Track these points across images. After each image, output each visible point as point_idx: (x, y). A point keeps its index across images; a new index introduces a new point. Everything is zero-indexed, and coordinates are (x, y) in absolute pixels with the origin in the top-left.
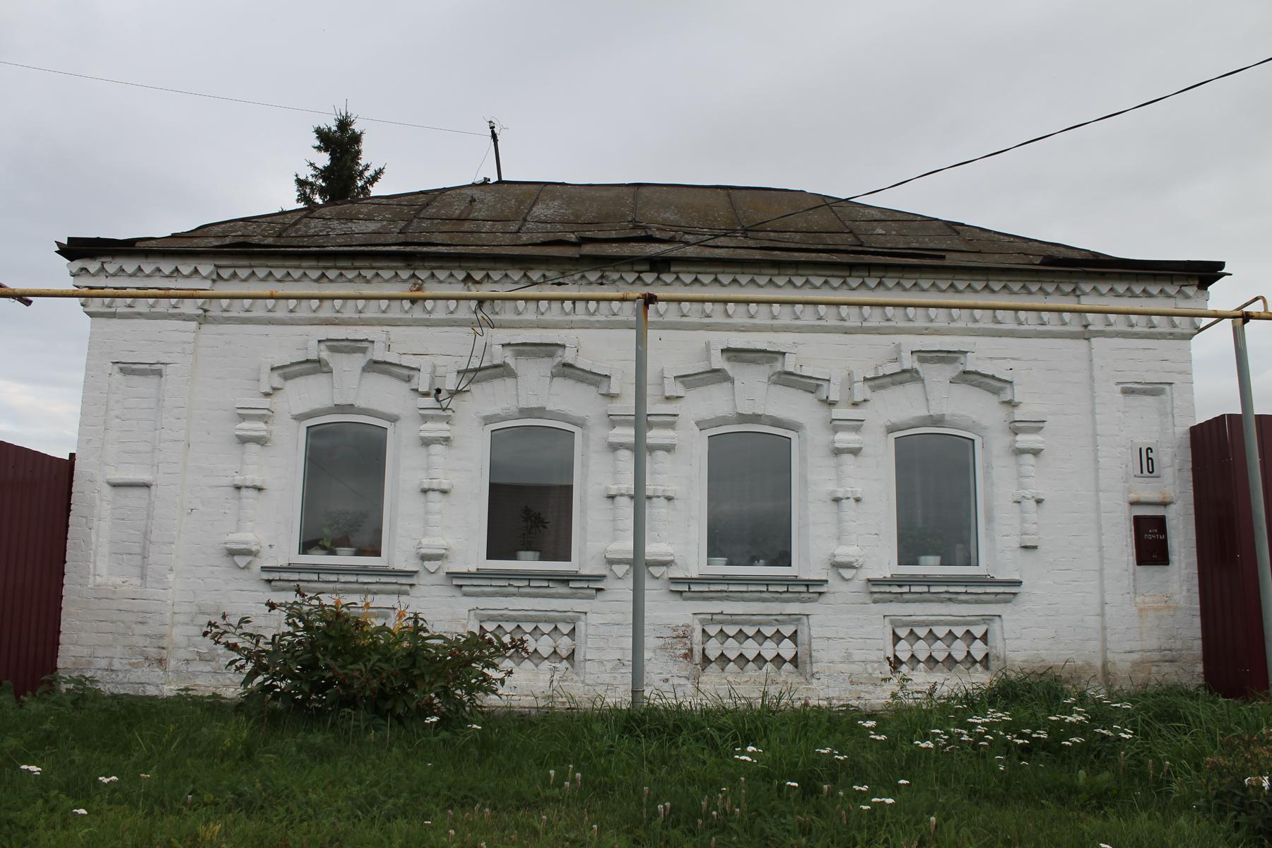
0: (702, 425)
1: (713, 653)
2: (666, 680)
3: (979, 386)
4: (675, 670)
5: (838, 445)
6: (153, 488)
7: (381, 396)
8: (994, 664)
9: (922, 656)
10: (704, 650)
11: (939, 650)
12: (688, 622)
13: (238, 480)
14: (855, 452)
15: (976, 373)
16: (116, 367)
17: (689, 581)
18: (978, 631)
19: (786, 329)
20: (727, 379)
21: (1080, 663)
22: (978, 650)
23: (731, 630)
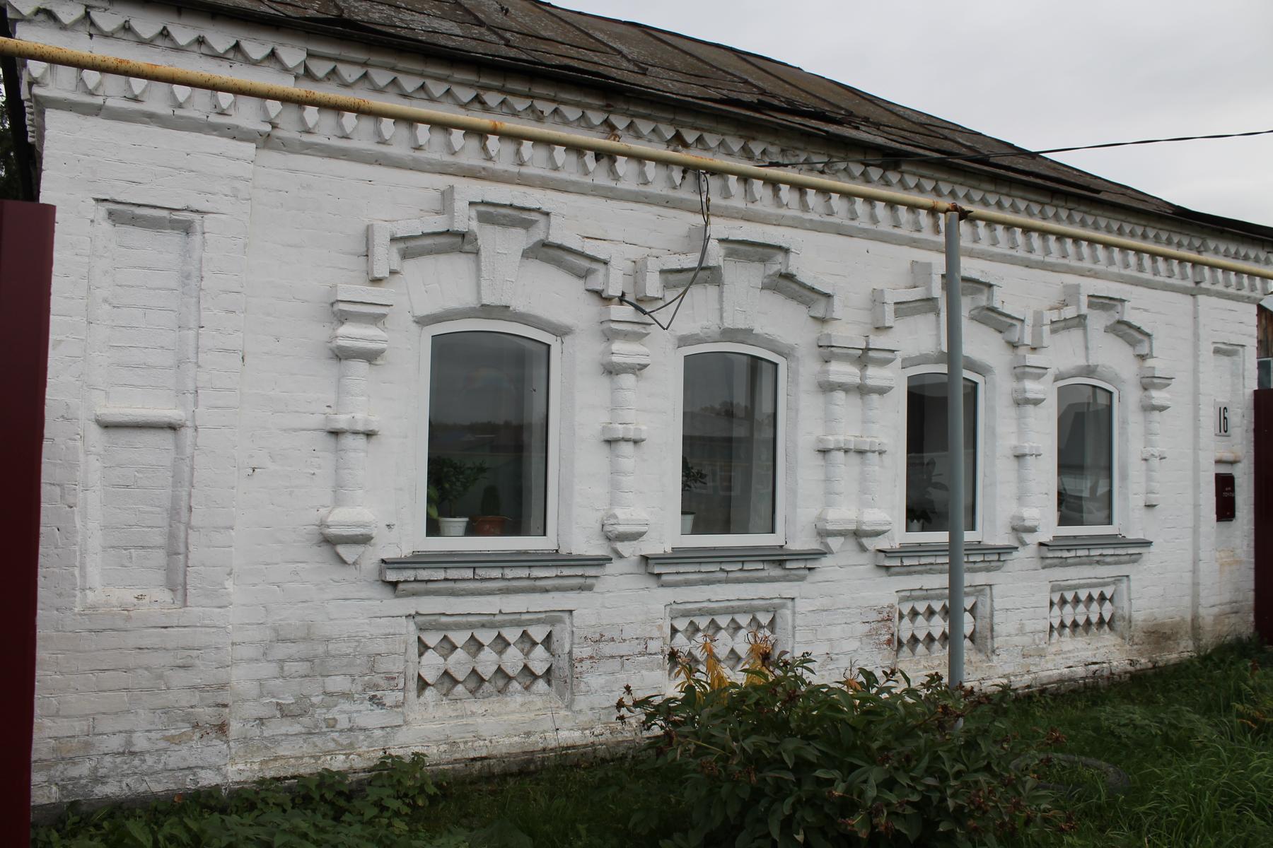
6: (188, 433)
7: (548, 296)
8: (1119, 625)
13: (342, 422)
16: (103, 209)
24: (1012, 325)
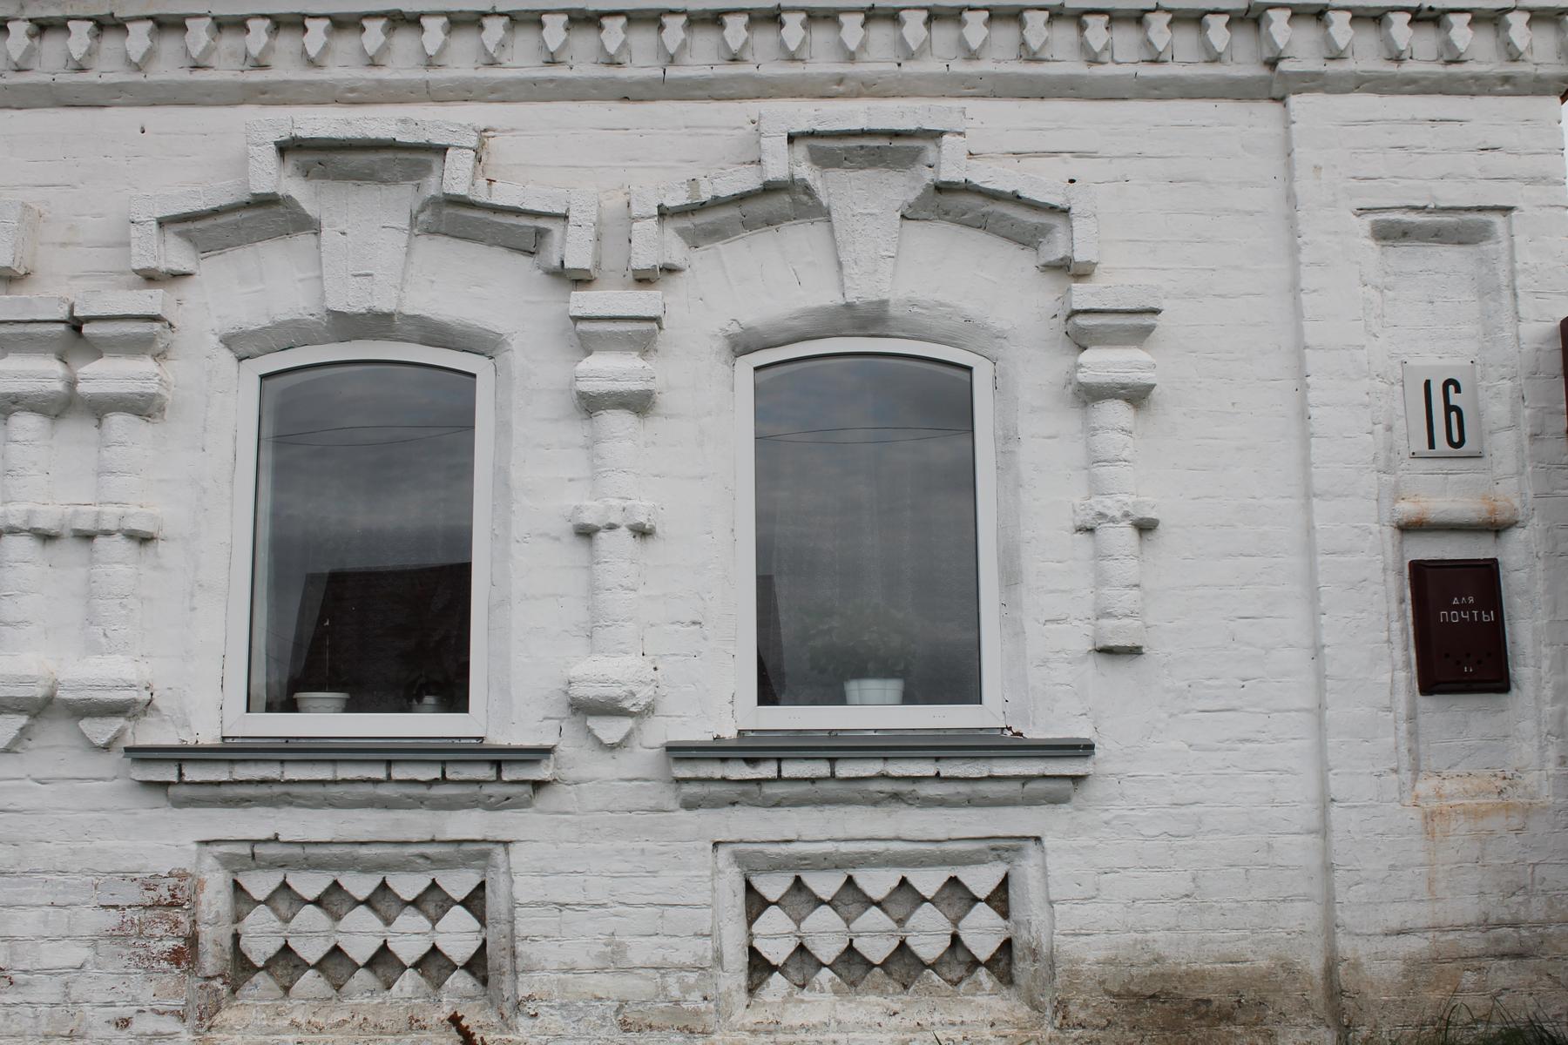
0: (240, 345)
1: (260, 948)
2: (124, 1023)
3: (981, 224)
4: (146, 993)
5: (584, 386)
8: (1023, 968)
9: (827, 950)
10: (236, 937)
11: (874, 934)
12: (185, 862)
14: (639, 404)
15: (968, 189)
17: (182, 755)
18: (982, 880)
20: (305, 224)
21: (1263, 963)
23: (310, 885)
24: (541, 234)
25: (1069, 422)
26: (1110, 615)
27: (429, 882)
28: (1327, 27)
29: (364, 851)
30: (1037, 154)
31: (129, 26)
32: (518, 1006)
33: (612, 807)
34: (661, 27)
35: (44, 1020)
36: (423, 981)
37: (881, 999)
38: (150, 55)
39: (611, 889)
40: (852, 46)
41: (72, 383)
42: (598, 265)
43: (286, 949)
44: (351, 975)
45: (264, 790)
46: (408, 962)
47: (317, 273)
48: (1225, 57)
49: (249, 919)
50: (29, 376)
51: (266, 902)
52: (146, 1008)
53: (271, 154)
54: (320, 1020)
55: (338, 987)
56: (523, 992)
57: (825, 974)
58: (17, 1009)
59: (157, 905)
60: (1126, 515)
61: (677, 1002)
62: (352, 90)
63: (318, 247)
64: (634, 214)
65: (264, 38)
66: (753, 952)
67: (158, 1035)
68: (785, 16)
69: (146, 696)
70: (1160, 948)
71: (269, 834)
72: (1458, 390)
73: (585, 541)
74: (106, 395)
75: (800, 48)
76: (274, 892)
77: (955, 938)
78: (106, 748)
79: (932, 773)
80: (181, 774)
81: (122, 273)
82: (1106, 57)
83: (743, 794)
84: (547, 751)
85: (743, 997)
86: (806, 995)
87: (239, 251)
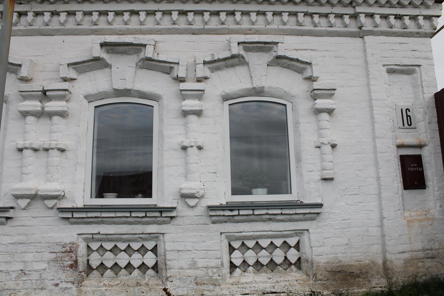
0: (89, 98)
1: (95, 263)
2: (57, 285)
3: (288, 67)
4: (63, 276)
5: (184, 108)
8: (304, 265)
9: (251, 261)
10: (88, 261)
11: (264, 257)
12: (74, 240)
14: (198, 113)
15: (285, 57)
17: (73, 210)
18: (292, 242)
19: (151, 32)
20: (107, 66)
21: (367, 262)
22: (293, 255)
23: (108, 246)
24: (171, 68)
25: (313, 119)
26: (326, 170)
27: (141, 245)
28: (374, 19)
29: (123, 236)
30: (301, 50)
31: (60, 14)
32: (167, 279)
33: (192, 223)
34: (203, 15)
35: (34, 285)
36: (140, 272)
37: (266, 275)
38: (66, 21)
39: (193, 246)
40: (254, 20)
41: (43, 108)
42: (187, 77)
43: (102, 264)
44: (120, 271)
45: (96, 220)
46: (136, 267)
47: (111, 79)
48: (348, 26)
49: (92, 255)
50: (31, 106)
51: (96, 251)
52: (63, 281)
53: (99, 46)
54: (112, 283)
55: (116, 274)
56: (169, 275)
57: (251, 268)
58: (27, 281)
59: (66, 252)
60: (329, 143)
61: (211, 277)
62: (120, 31)
63: (111, 72)
64: (197, 63)
65: (97, 17)
66: (231, 263)
67: (66, 288)
68: (236, 13)
69: (63, 194)
70: (341, 259)
71: (97, 232)
72: (409, 111)
73: (184, 150)
74: (53, 111)
75: (240, 21)
76: (99, 248)
77: (286, 257)
78: (52, 208)
79: (280, 213)
80: (73, 215)
81: (57, 79)
82: (318, 25)
83: (229, 219)
84: (175, 208)
85: (228, 275)
86: (246, 274)
87: (89, 73)
